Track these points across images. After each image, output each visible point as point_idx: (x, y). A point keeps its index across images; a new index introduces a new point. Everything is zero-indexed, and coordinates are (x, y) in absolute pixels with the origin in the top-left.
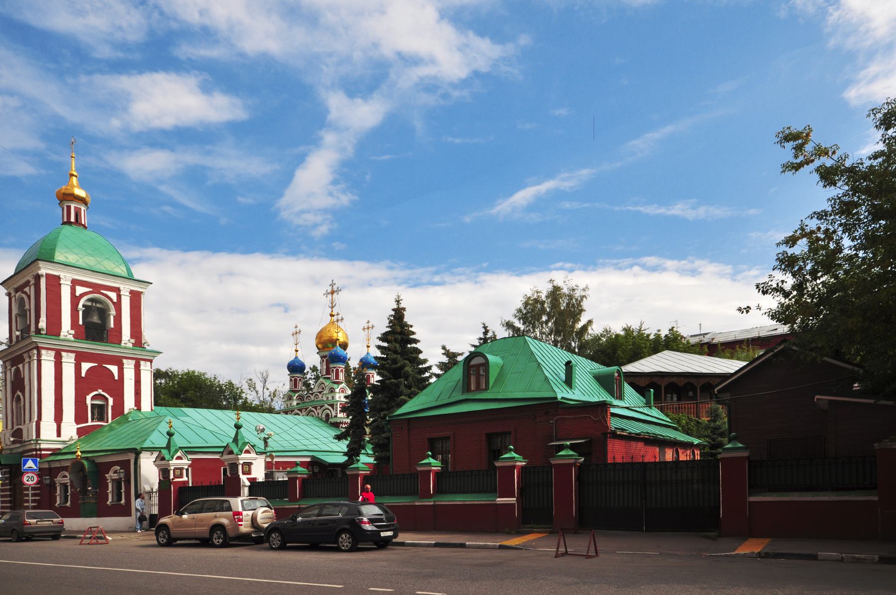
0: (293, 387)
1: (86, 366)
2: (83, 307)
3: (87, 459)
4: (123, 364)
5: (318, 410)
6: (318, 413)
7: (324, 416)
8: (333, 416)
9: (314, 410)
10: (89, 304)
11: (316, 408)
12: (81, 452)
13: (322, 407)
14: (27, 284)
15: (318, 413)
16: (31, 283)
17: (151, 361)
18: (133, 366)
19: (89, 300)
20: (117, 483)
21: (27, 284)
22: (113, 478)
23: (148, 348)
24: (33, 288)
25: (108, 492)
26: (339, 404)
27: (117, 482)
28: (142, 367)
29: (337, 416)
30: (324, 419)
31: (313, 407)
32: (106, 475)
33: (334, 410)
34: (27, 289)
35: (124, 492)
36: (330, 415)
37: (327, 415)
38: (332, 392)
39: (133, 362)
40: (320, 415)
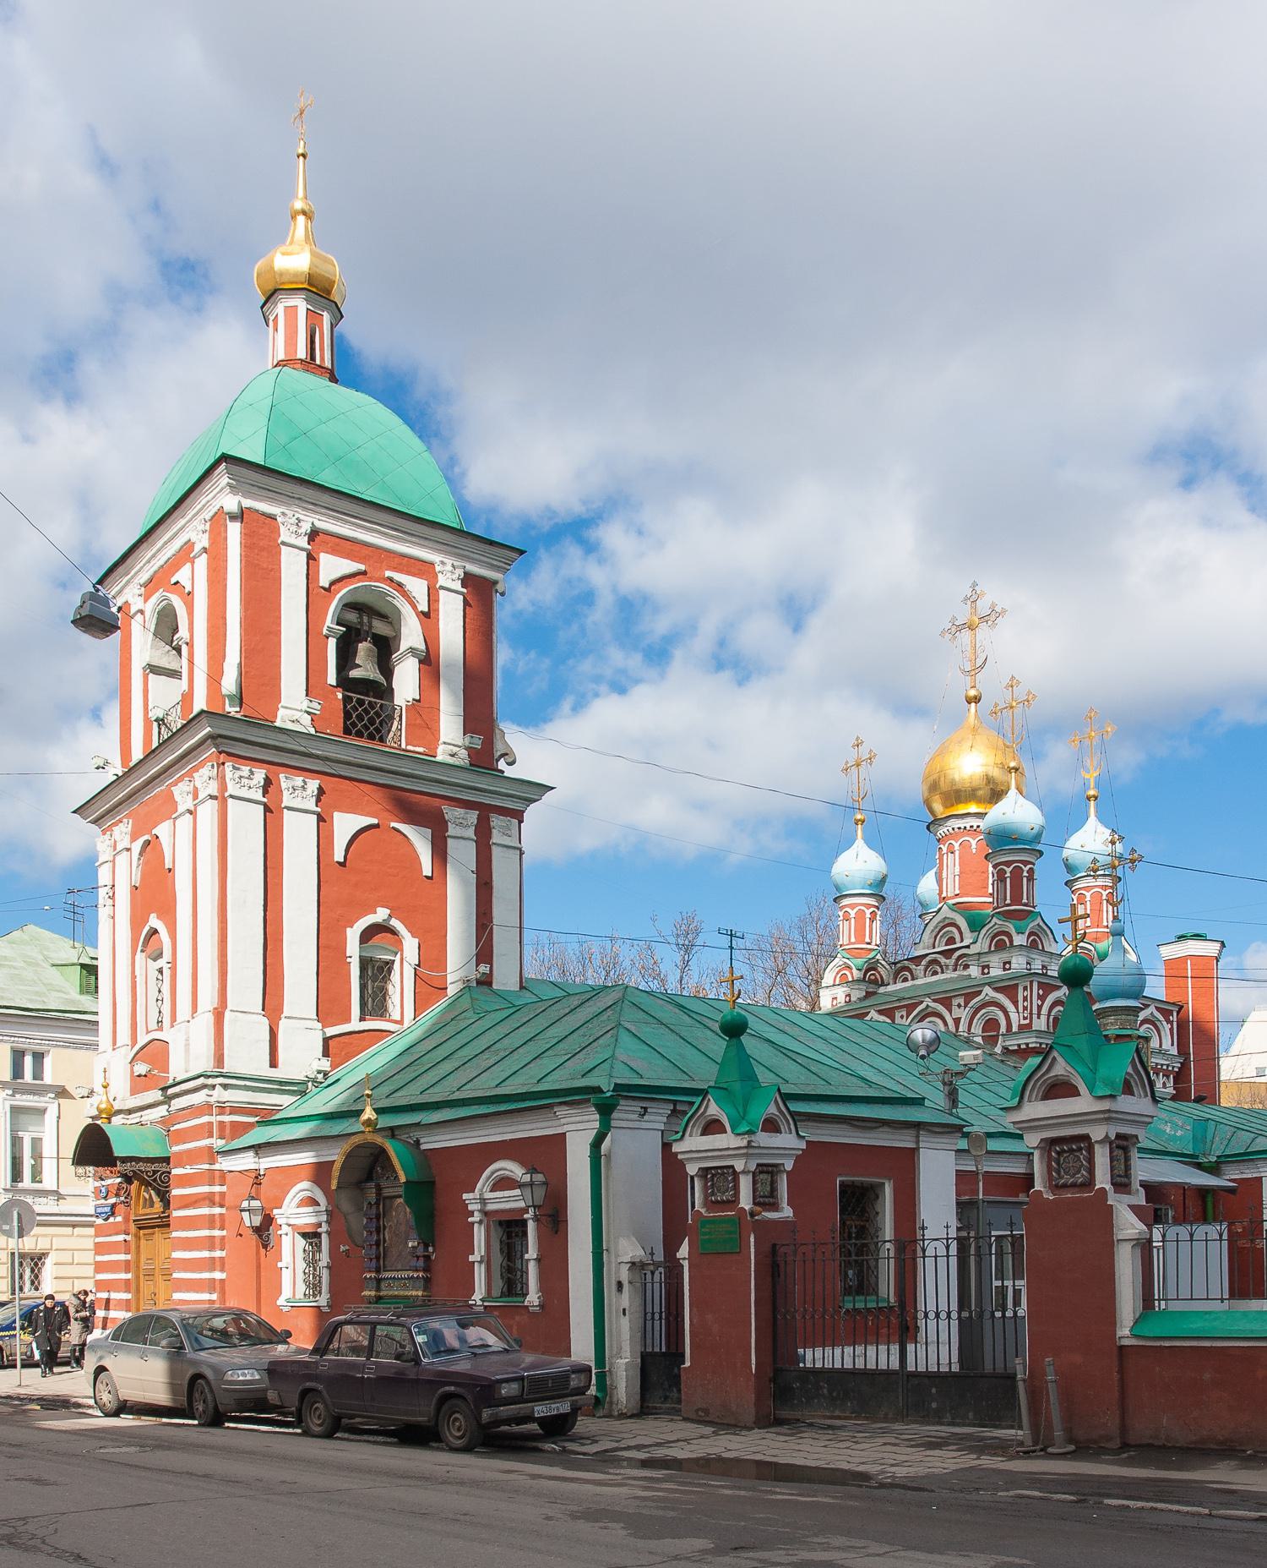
0: (853, 940)
1: (346, 824)
2: (338, 624)
3: (392, 1132)
4: (446, 822)
5: (955, 1008)
6: (957, 1021)
7: (977, 1028)
8: (1015, 1029)
9: (940, 1008)
10: (352, 617)
11: (947, 1002)
12: (378, 1111)
13: (969, 997)
14: (185, 555)
15: (957, 1021)
16: (197, 548)
17: (518, 816)
18: (470, 833)
19: (349, 606)
20: (510, 1228)
21: (185, 555)
22: (490, 1207)
23: (510, 772)
24: (202, 563)
25: (471, 1258)
26: (1035, 986)
27: (501, 1223)
28: (496, 837)
29: (1030, 1025)
30: (979, 1040)
31: (934, 1001)
32: (465, 1196)
33: (1015, 1003)
34: (182, 576)
35: (538, 1260)
36: (1003, 1023)
37: (992, 1024)
38: (1001, 946)
39: (473, 816)
40: (963, 1027)
